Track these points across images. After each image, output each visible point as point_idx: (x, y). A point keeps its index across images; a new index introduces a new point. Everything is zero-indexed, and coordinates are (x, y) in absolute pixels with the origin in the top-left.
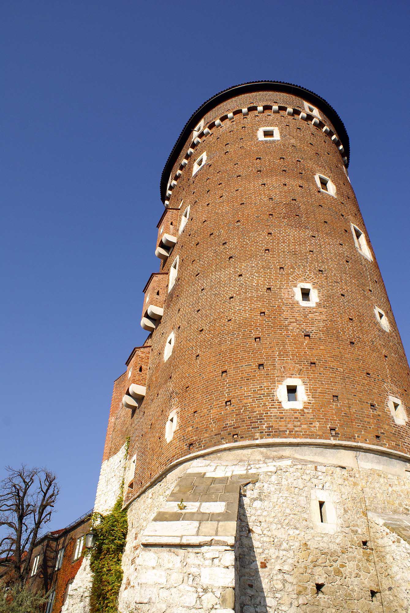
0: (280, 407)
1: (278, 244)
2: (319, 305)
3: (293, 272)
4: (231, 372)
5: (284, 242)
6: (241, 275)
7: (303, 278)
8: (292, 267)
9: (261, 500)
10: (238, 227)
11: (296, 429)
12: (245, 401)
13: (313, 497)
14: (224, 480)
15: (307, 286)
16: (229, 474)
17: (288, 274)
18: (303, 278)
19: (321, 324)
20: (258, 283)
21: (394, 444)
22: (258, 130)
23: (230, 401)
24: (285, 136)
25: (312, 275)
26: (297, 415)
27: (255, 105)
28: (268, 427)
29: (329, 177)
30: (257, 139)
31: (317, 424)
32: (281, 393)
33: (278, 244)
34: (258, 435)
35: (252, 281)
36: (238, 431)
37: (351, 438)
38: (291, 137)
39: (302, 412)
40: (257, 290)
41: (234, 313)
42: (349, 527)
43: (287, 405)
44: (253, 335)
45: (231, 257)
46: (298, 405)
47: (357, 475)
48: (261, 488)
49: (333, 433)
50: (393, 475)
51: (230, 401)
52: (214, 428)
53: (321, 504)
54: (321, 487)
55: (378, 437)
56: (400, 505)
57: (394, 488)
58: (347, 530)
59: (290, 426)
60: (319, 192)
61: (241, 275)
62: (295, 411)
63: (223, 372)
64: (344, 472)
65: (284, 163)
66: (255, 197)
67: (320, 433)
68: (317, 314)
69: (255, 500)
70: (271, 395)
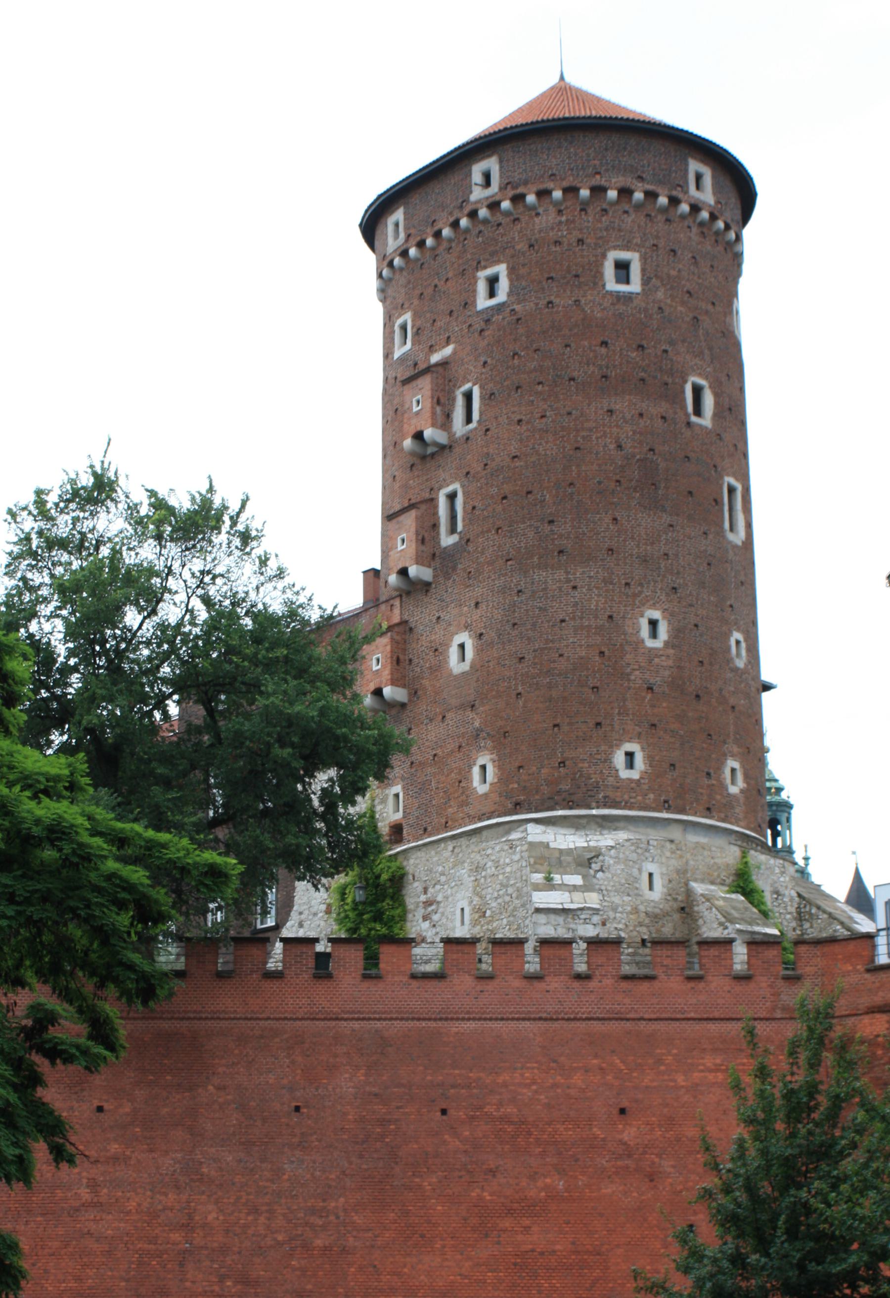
0: (617, 776)
1: (625, 541)
2: (667, 644)
3: (641, 592)
4: (565, 728)
5: (632, 538)
6: (575, 588)
7: (651, 602)
8: (641, 585)
9: (603, 871)
10: (572, 494)
11: (632, 800)
12: (581, 765)
13: (644, 869)
14: (569, 852)
15: (656, 614)
16: (572, 846)
17: (635, 595)
18: (651, 602)
19: (667, 673)
20: (597, 605)
21: (722, 815)
22: (604, 256)
23: (563, 762)
24: (650, 279)
25: (663, 598)
26: (633, 785)
27: (603, 183)
28: (605, 797)
29: (706, 378)
30: (604, 286)
31: (651, 796)
32: (619, 759)
33: (625, 541)
34: (594, 804)
35: (589, 600)
36: (574, 798)
37: (682, 811)
38: (659, 284)
39: (638, 782)
40: (596, 617)
41: (567, 646)
42: (670, 895)
43: (624, 774)
44: (591, 683)
45: (561, 552)
46: (635, 775)
47: (684, 848)
48: (603, 861)
49: (666, 805)
50: (717, 847)
51: (563, 762)
52: (545, 790)
53: (651, 875)
54: (651, 859)
55: (708, 809)
56: (719, 876)
57: (716, 860)
58: (669, 898)
59: (626, 797)
60: (689, 424)
61: (575, 588)
62: (631, 780)
63: (555, 726)
64: (673, 846)
65: (643, 360)
66: (597, 438)
67: (654, 805)
68: (663, 658)
69: (598, 871)
70: (608, 760)
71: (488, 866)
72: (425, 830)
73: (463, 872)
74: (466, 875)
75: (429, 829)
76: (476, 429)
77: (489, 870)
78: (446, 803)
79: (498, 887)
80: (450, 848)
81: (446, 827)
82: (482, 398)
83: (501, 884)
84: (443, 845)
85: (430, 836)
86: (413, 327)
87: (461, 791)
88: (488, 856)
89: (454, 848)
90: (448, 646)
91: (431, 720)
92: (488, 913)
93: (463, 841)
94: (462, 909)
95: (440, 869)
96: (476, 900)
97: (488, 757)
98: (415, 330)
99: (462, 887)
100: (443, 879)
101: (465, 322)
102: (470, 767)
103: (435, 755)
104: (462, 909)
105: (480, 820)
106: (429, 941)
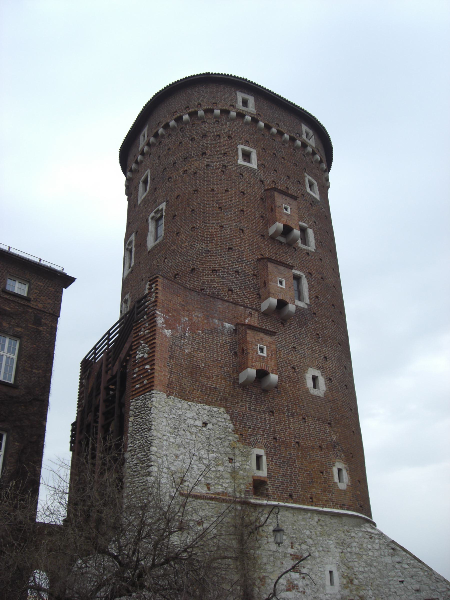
71: (352, 545)
72: (291, 496)
73: (331, 543)
74: (333, 546)
75: (295, 497)
76: (313, 253)
77: (354, 549)
78: (309, 483)
79: (363, 564)
80: (316, 519)
81: (311, 501)
82: (316, 239)
83: (366, 562)
84: (309, 514)
85: (295, 502)
86: (258, 160)
87: (323, 480)
88: (352, 537)
89: (319, 520)
90: (305, 371)
91: (292, 415)
92: (356, 582)
93: (327, 519)
94: (331, 572)
95: (308, 533)
96: (344, 568)
97: (344, 465)
98: (260, 163)
99: (329, 553)
100: (310, 541)
101: (299, 190)
102: (331, 468)
103: (297, 443)
104: (331, 572)
105: (341, 507)
106: (301, 589)
